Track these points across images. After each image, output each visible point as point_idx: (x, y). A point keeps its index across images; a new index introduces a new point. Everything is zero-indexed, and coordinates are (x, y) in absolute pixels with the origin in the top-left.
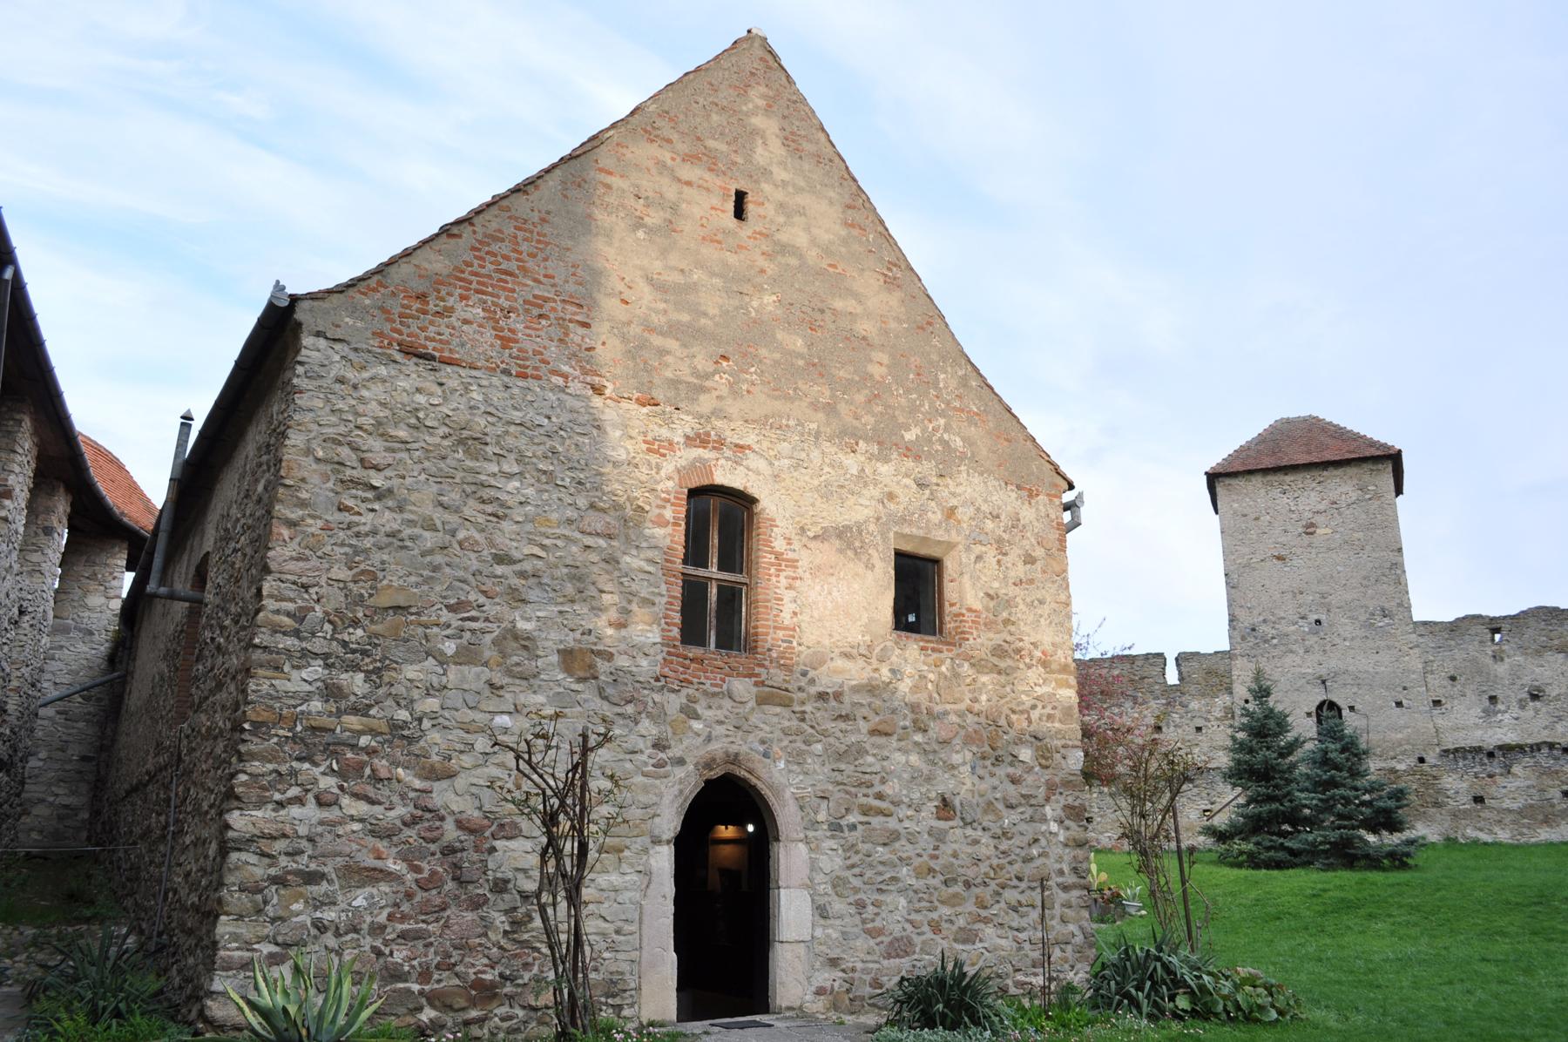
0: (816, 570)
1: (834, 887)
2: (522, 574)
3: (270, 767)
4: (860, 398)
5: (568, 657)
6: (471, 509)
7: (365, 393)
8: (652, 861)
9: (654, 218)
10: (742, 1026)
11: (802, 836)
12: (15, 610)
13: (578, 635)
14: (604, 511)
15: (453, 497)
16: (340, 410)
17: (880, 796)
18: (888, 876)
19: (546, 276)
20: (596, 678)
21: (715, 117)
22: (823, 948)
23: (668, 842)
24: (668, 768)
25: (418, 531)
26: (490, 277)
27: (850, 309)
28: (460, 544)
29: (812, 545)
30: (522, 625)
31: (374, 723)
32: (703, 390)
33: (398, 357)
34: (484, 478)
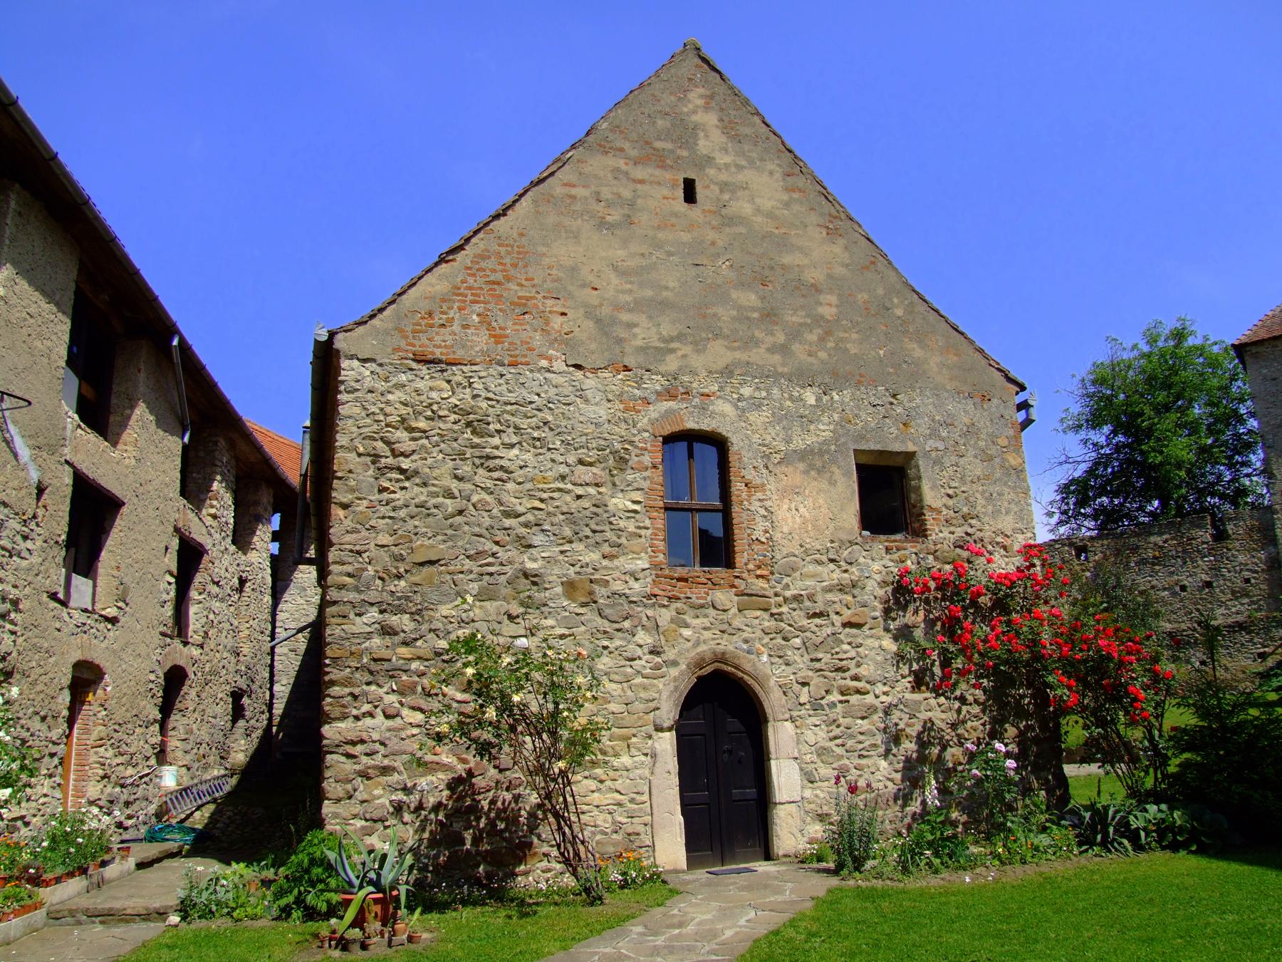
0: (785, 493)
1: (819, 755)
2: (526, 525)
3: (347, 690)
4: (813, 337)
5: (570, 587)
6: (482, 476)
7: (390, 397)
8: (657, 745)
10: (739, 872)
11: (787, 716)
12: (236, 581)
13: (577, 568)
14: (591, 464)
15: (466, 469)
16: (373, 413)
17: (856, 678)
18: (867, 744)
19: (527, 280)
20: (595, 602)
21: (660, 122)
22: (812, 806)
23: (670, 729)
24: (664, 669)
25: (440, 500)
26: (481, 288)
27: (796, 262)
28: (474, 506)
29: (778, 470)
30: (530, 565)
31: (421, 653)
33: (414, 365)
34: (488, 450)
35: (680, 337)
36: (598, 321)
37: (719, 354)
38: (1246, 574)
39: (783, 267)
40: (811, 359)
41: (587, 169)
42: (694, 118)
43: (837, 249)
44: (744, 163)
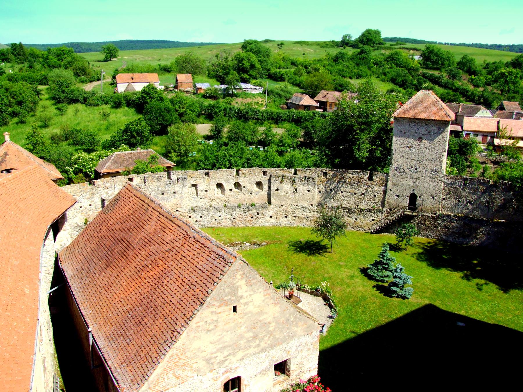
9: (212, 327)
32: (227, 360)
35: (230, 355)
37: (240, 354)
38: (376, 194)
39: (260, 321)
40: (266, 345)
41: (203, 315)
42: (238, 284)
43: (277, 308)
44: (252, 293)
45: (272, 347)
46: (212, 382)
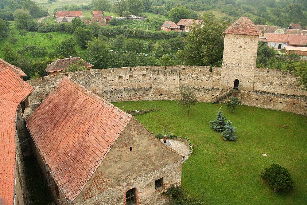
32: (128, 178)
35: (129, 175)
36: (116, 179)
37: (135, 175)
39: (147, 155)
41: (112, 153)
43: (156, 148)
45: (154, 170)
46: (119, 191)
